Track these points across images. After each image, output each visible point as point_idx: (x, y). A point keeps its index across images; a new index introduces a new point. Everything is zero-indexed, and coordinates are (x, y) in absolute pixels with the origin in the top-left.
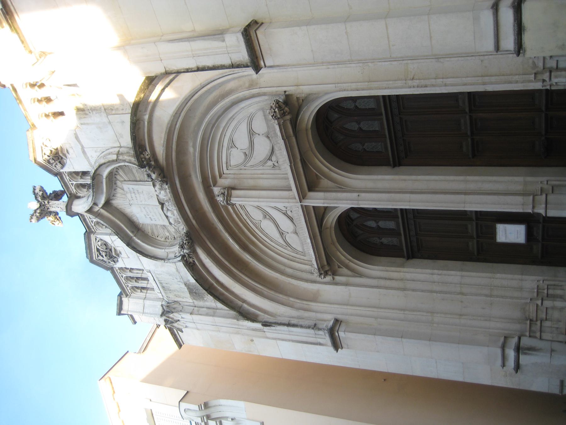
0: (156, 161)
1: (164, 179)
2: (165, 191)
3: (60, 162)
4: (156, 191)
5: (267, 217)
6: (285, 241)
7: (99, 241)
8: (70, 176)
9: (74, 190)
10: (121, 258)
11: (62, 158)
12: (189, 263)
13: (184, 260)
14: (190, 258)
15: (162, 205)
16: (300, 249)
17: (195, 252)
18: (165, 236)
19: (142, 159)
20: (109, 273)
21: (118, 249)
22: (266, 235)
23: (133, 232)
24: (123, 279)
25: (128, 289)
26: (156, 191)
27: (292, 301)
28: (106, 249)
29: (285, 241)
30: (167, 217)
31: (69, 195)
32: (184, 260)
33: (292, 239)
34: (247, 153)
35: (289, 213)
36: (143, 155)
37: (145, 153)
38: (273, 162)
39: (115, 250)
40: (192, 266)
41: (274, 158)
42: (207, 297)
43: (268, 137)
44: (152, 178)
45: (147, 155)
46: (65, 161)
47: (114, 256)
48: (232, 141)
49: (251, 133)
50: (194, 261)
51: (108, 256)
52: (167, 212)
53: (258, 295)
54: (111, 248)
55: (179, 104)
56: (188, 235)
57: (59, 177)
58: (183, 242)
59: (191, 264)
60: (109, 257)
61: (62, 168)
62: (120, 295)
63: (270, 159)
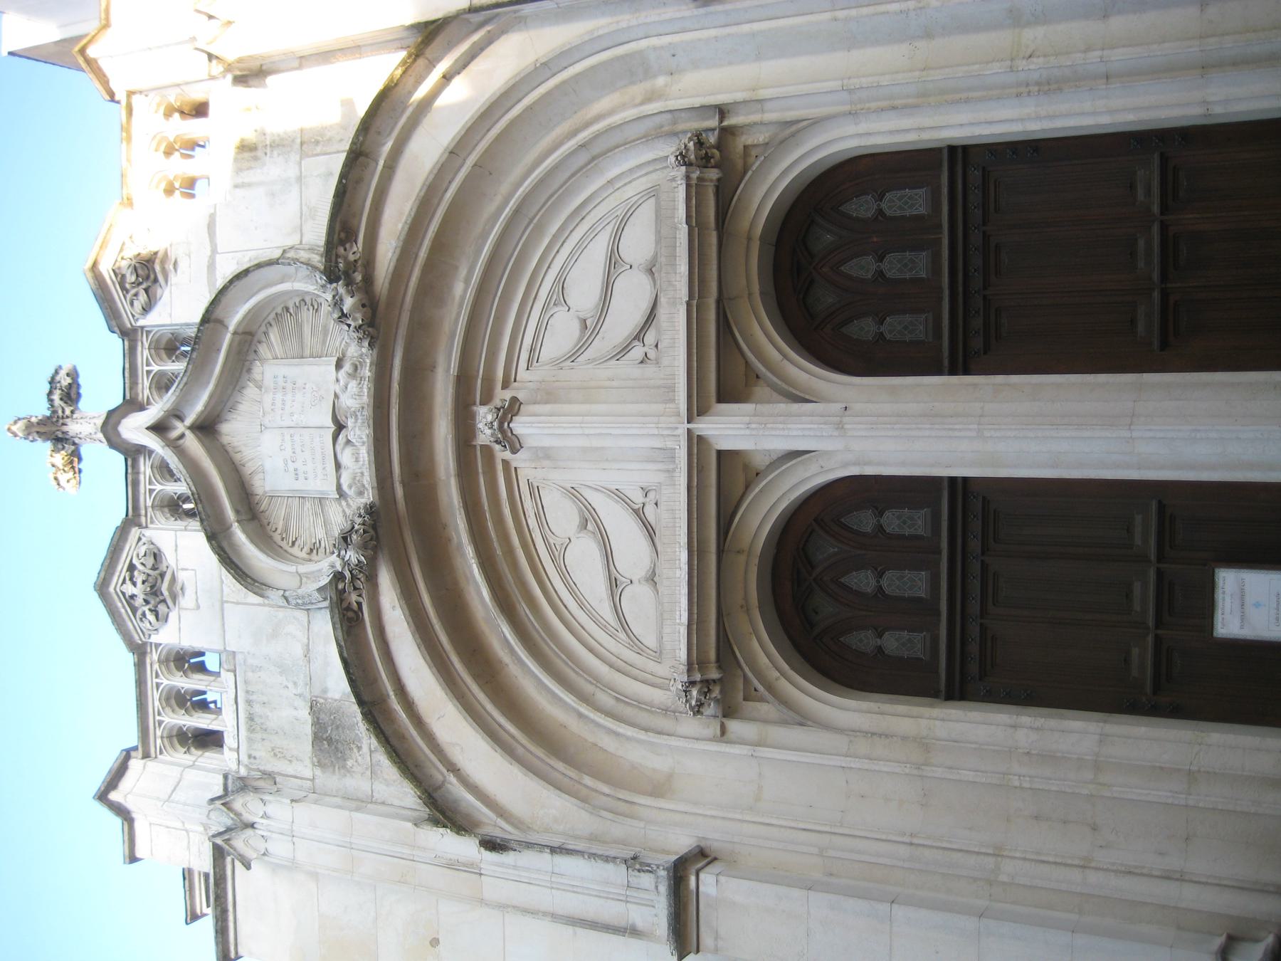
0: (369, 280)
1: (370, 329)
2: (360, 383)
3: (146, 290)
4: (338, 380)
6: (617, 610)
7: (144, 544)
8: (153, 351)
9: (147, 392)
10: (179, 608)
11: (156, 280)
12: (345, 605)
13: (336, 588)
14: (355, 589)
15: (340, 427)
16: (650, 641)
17: (372, 579)
18: (314, 541)
19: (337, 256)
20: (129, 659)
21: (181, 576)
23: (237, 512)
24: (157, 696)
25: (159, 733)
26: (338, 380)
27: (587, 787)
29: (617, 610)
30: (338, 466)
31: (128, 397)
32: (336, 588)
33: (638, 601)
34: (588, 323)
35: (650, 512)
36: (345, 250)
37: (351, 247)
38: (646, 349)
39: (173, 579)
40: (350, 620)
41: (650, 337)
42: (357, 755)
43: (650, 272)
44: (342, 310)
45: (354, 253)
46: (159, 291)
47: (162, 594)
48: (561, 284)
49: (614, 261)
50: (359, 604)
51: (150, 585)
52: (343, 449)
53: (497, 748)
54: (165, 569)
55: (472, 117)
56: (374, 516)
57: (126, 343)
58: (353, 527)
59: (350, 614)
60: (152, 587)
61: (146, 310)
62: (127, 755)
63: (639, 336)
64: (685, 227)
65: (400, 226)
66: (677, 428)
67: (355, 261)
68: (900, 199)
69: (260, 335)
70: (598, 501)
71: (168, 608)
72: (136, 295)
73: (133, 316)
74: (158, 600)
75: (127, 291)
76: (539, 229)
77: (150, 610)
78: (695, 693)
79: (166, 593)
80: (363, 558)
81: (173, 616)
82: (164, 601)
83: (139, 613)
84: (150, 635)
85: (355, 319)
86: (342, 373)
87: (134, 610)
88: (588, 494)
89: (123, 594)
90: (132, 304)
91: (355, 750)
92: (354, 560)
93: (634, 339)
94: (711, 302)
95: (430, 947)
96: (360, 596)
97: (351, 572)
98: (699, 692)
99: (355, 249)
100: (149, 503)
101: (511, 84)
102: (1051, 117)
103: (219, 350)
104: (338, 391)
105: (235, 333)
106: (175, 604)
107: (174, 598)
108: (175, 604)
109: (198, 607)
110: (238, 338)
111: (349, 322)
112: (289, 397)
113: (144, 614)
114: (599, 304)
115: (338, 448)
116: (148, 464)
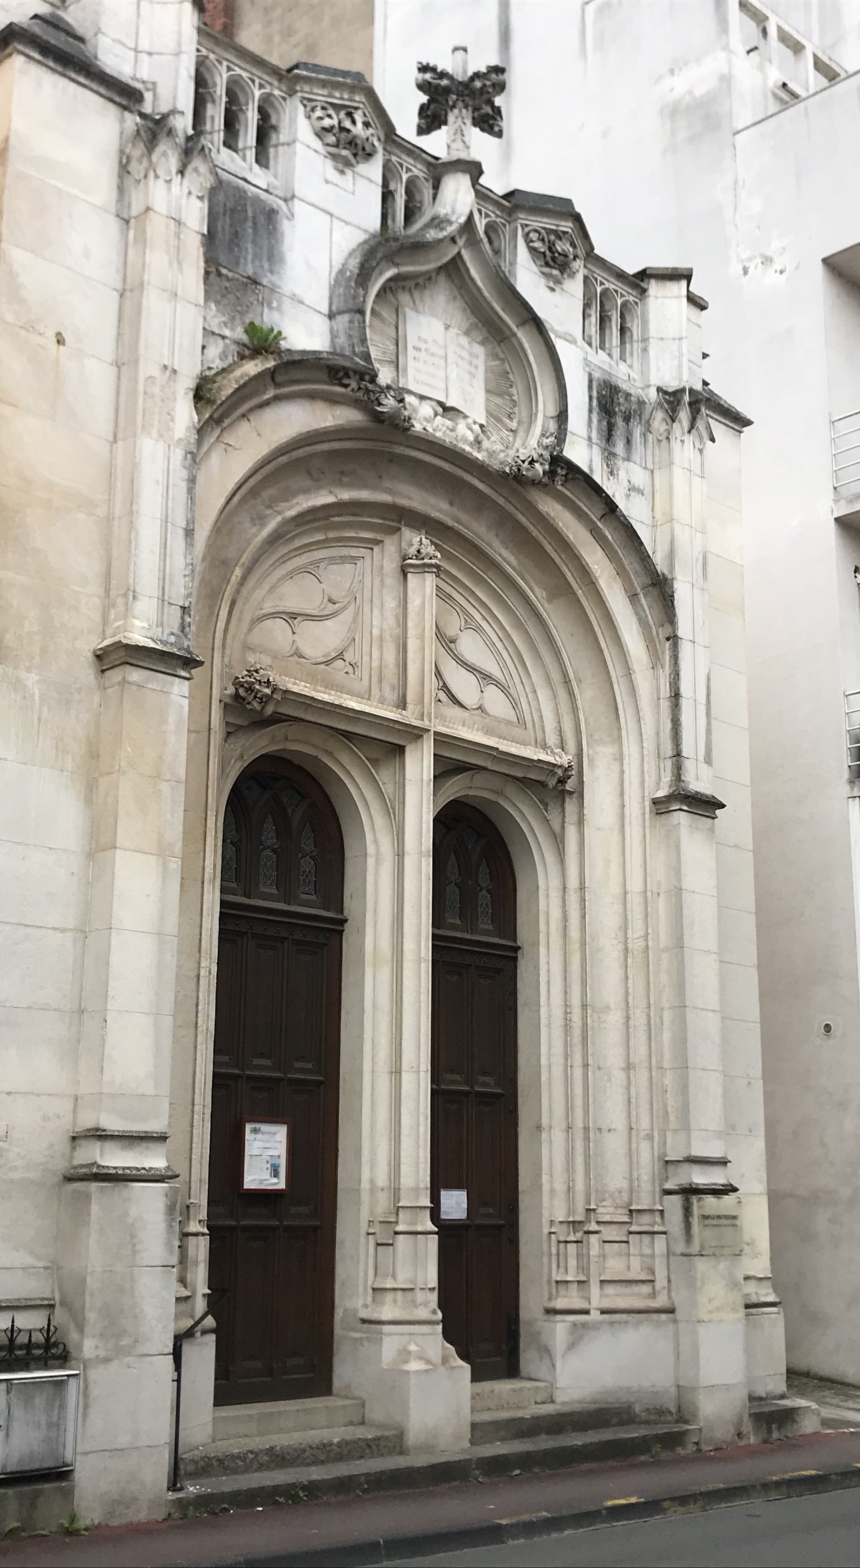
3: (544, 254)
4: (475, 423)
5: (331, 608)
11: (547, 264)
12: (351, 373)
13: (369, 374)
14: (359, 388)
15: (447, 410)
16: (256, 637)
17: (356, 404)
22: (291, 575)
24: (245, 75)
25: (212, 56)
28: (364, 149)
30: (422, 398)
34: (453, 645)
43: (480, 708)
44: (537, 462)
46: (539, 263)
47: (345, 148)
48: (479, 629)
49: (485, 677)
52: (433, 409)
59: (341, 374)
60: (356, 145)
64: (536, 758)
65: (561, 525)
66: (430, 721)
67: (554, 481)
68: (487, 904)
69: (498, 350)
70: (347, 616)
71: (328, 145)
72: (543, 240)
73: (527, 225)
74: (342, 142)
75: (548, 235)
76: (519, 625)
77: (332, 127)
78: (268, 691)
79: (345, 153)
80: (385, 410)
81: (317, 144)
82: (337, 146)
83: (331, 112)
84: (305, 106)
85: (527, 470)
86: (476, 428)
87: (337, 107)
88: (351, 609)
89: (357, 108)
90: (536, 231)
91: (224, 319)
92: (384, 401)
93: (444, 683)
94: (489, 765)
95: (58, 330)
96: (353, 390)
97: (373, 391)
98: (266, 695)
99: (560, 483)
100: (394, 159)
101: (625, 647)
102: (549, 1026)
103: (504, 310)
104: (470, 421)
105: (515, 335)
106: (329, 153)
107: (334, 157)
108: (329, 153)
109: (327, 182)
110: (507, 333)
111: (526, 463)
112: (467, 367)
113: (329, 116)
114: (463, 656)
115: (434, 404)
116: (421, 175)
